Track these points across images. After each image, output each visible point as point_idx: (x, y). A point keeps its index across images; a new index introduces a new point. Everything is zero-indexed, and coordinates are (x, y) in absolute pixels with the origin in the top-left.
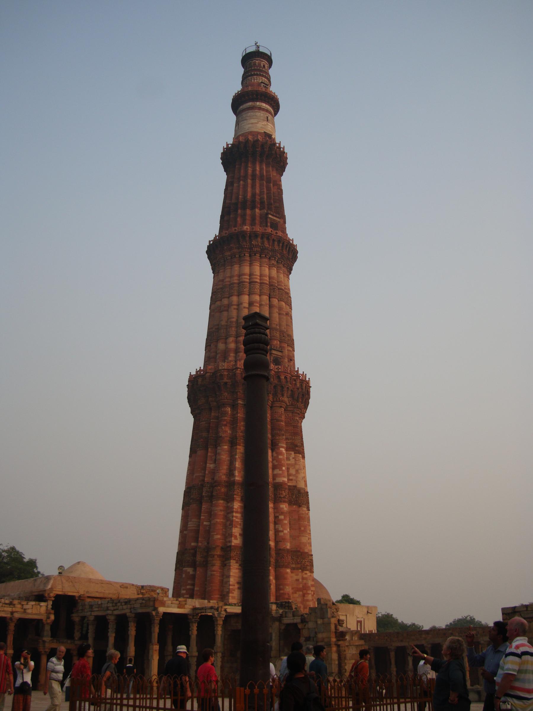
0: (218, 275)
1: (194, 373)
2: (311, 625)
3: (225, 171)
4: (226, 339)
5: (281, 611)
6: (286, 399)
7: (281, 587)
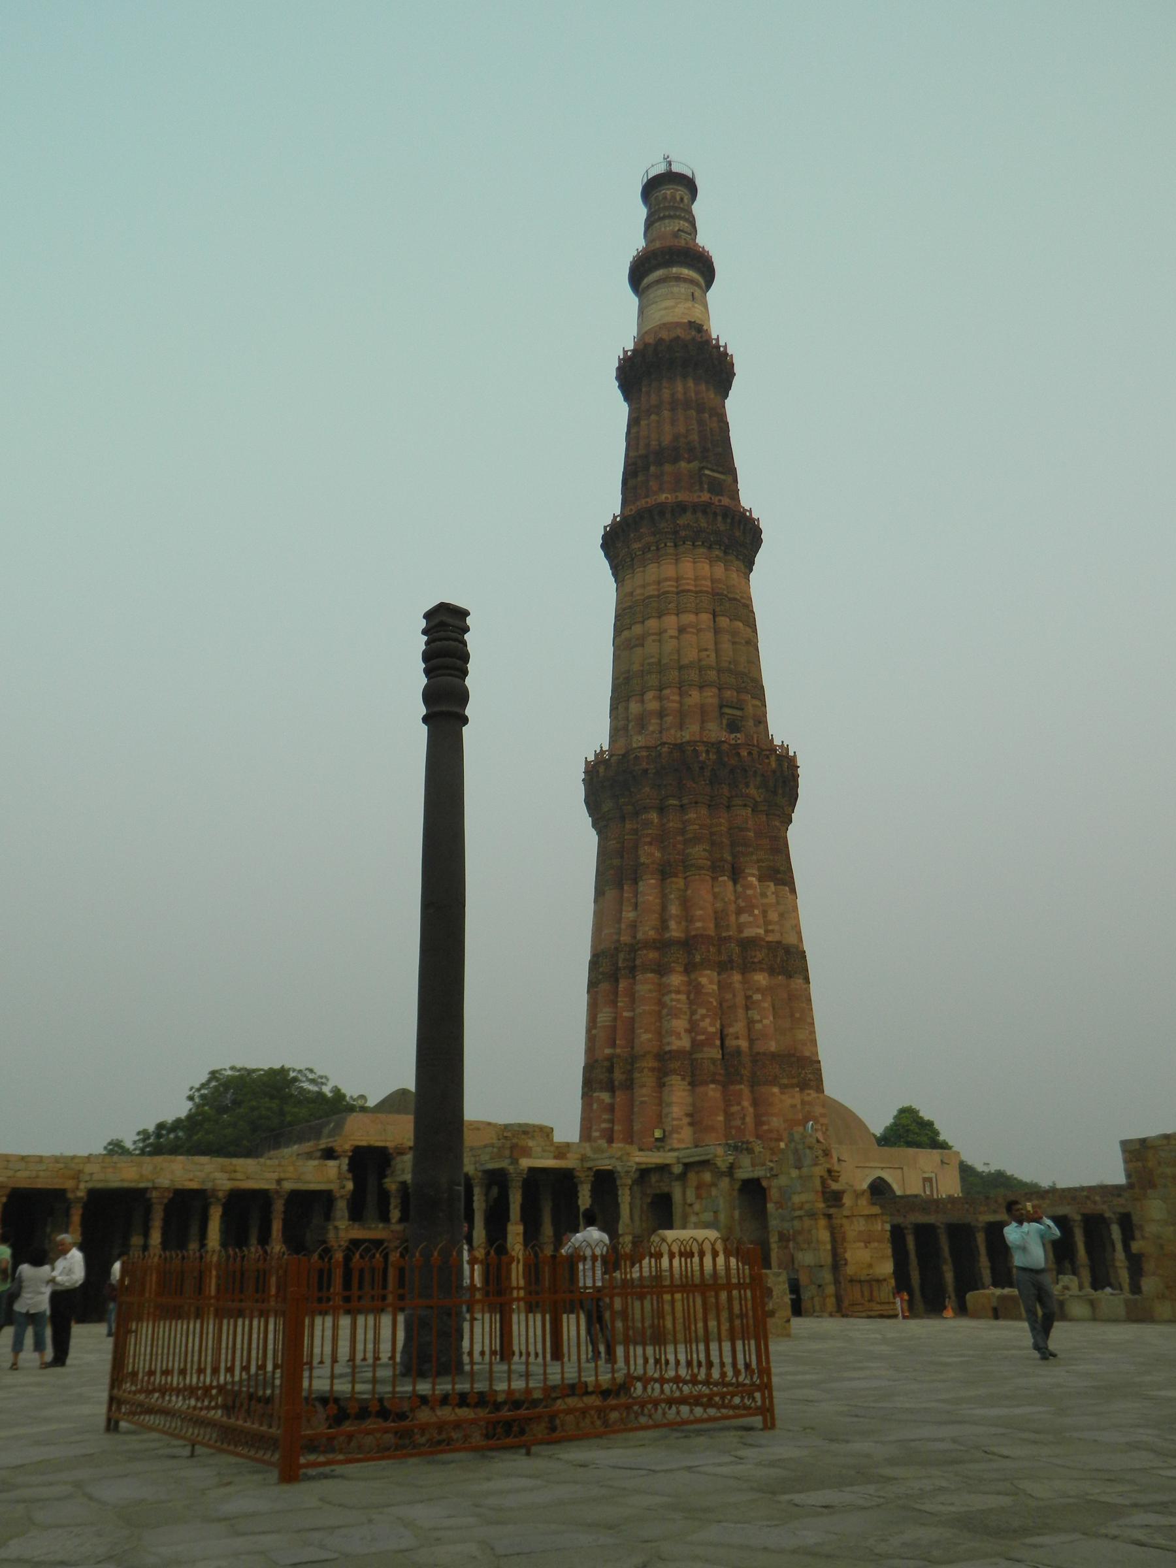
1: (591, 758)
2: (783, 1181)
3: (626, 398)
4: (642, 695)
5: (731, 1159)
6: (752, 791)
7: (764, 1119)
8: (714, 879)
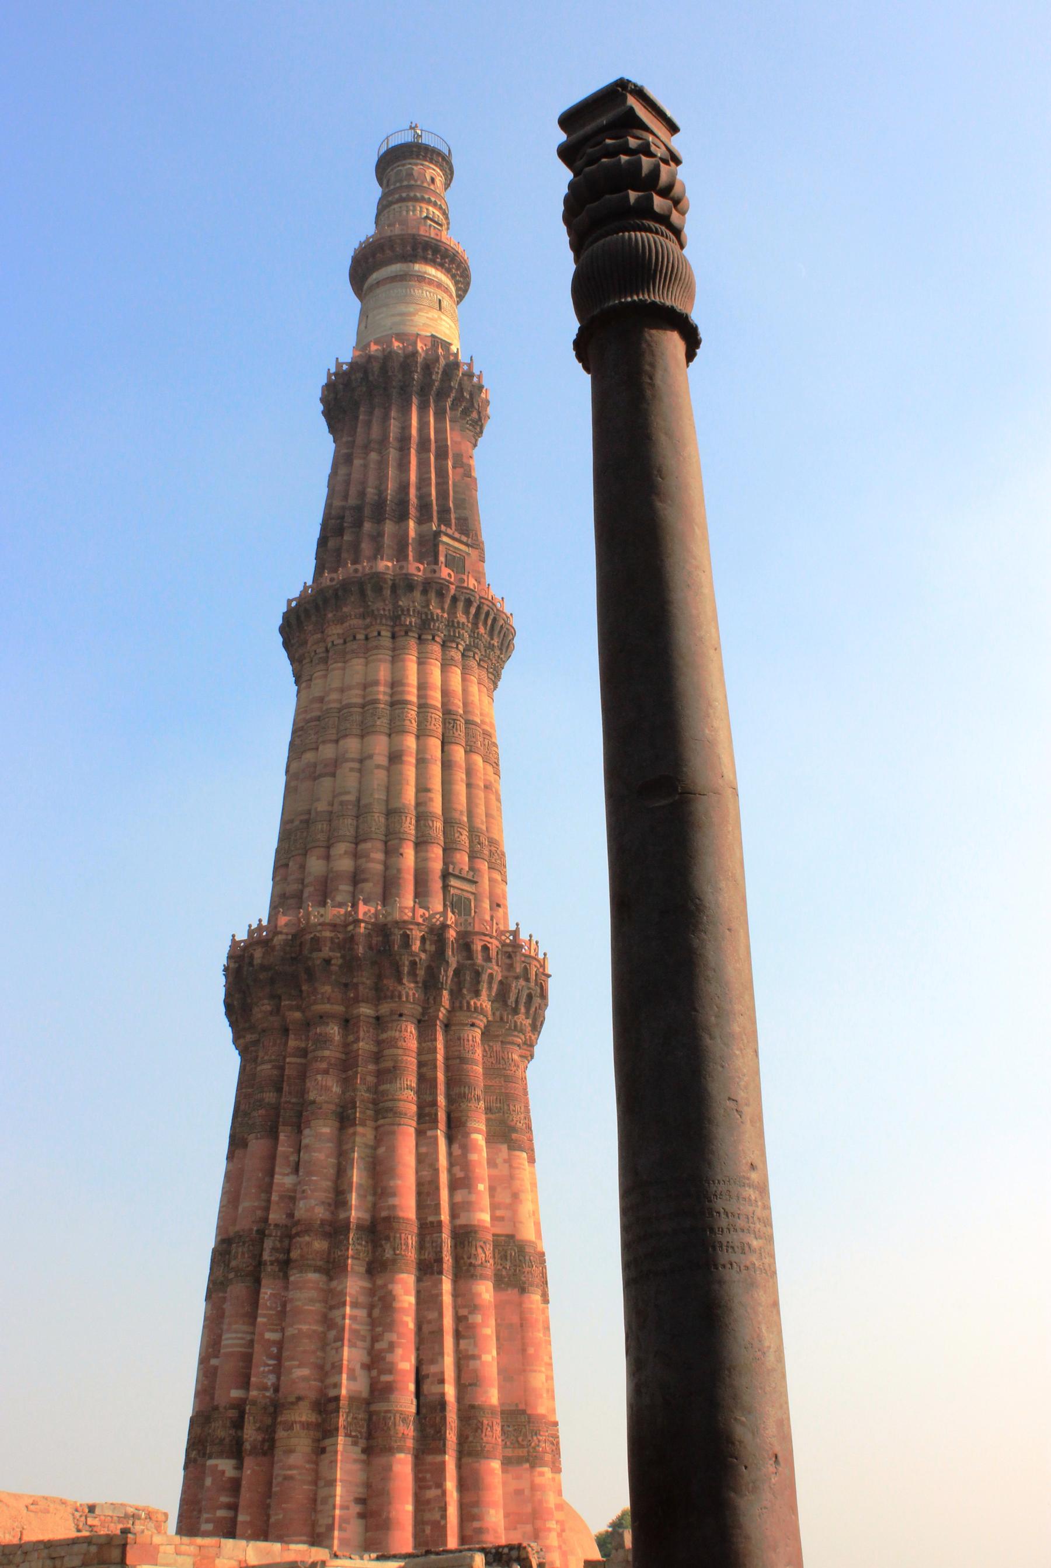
0: (309, 687)
1: (242, 936)
3: (332, 429)
4: (328, 847)
8: (420, 1133)
